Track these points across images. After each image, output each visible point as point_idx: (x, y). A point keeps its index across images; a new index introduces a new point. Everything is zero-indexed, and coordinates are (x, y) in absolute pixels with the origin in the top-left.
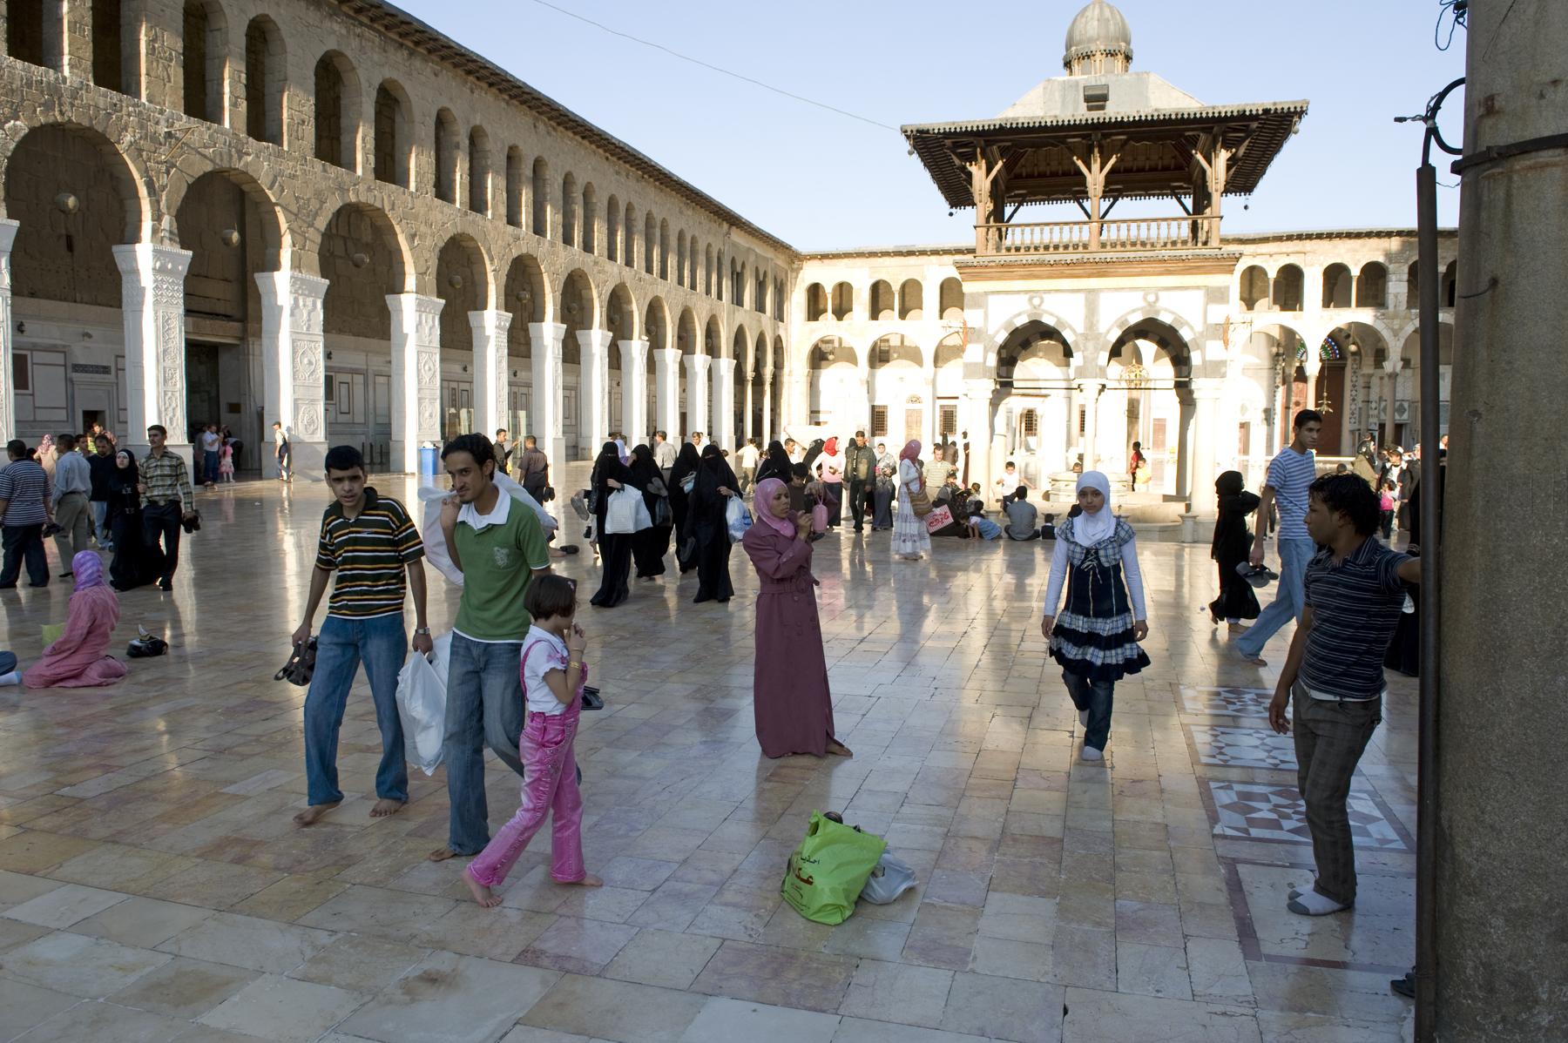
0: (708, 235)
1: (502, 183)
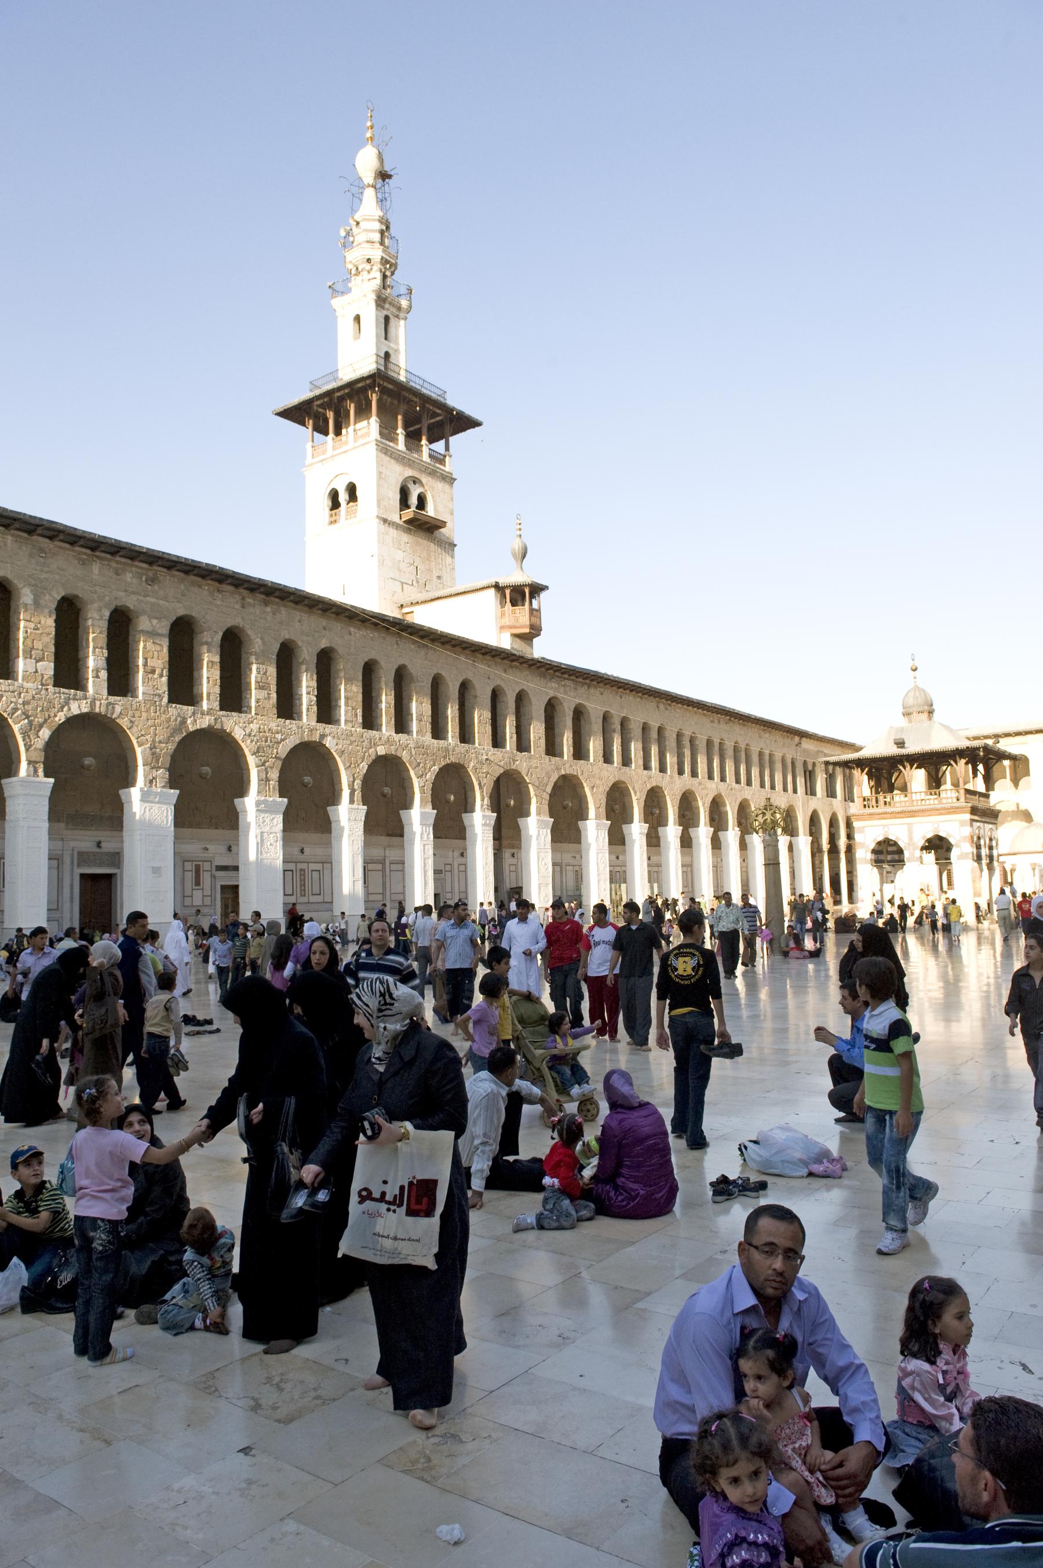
0: (781, 749)
1: (640, 746)
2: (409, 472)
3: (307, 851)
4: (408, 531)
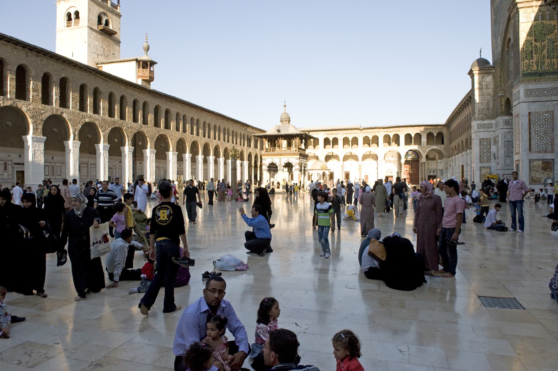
0: (240, 131)
1: (190, 126)
2: (102, 10)
3: (54, 158)
4: (101, 34)
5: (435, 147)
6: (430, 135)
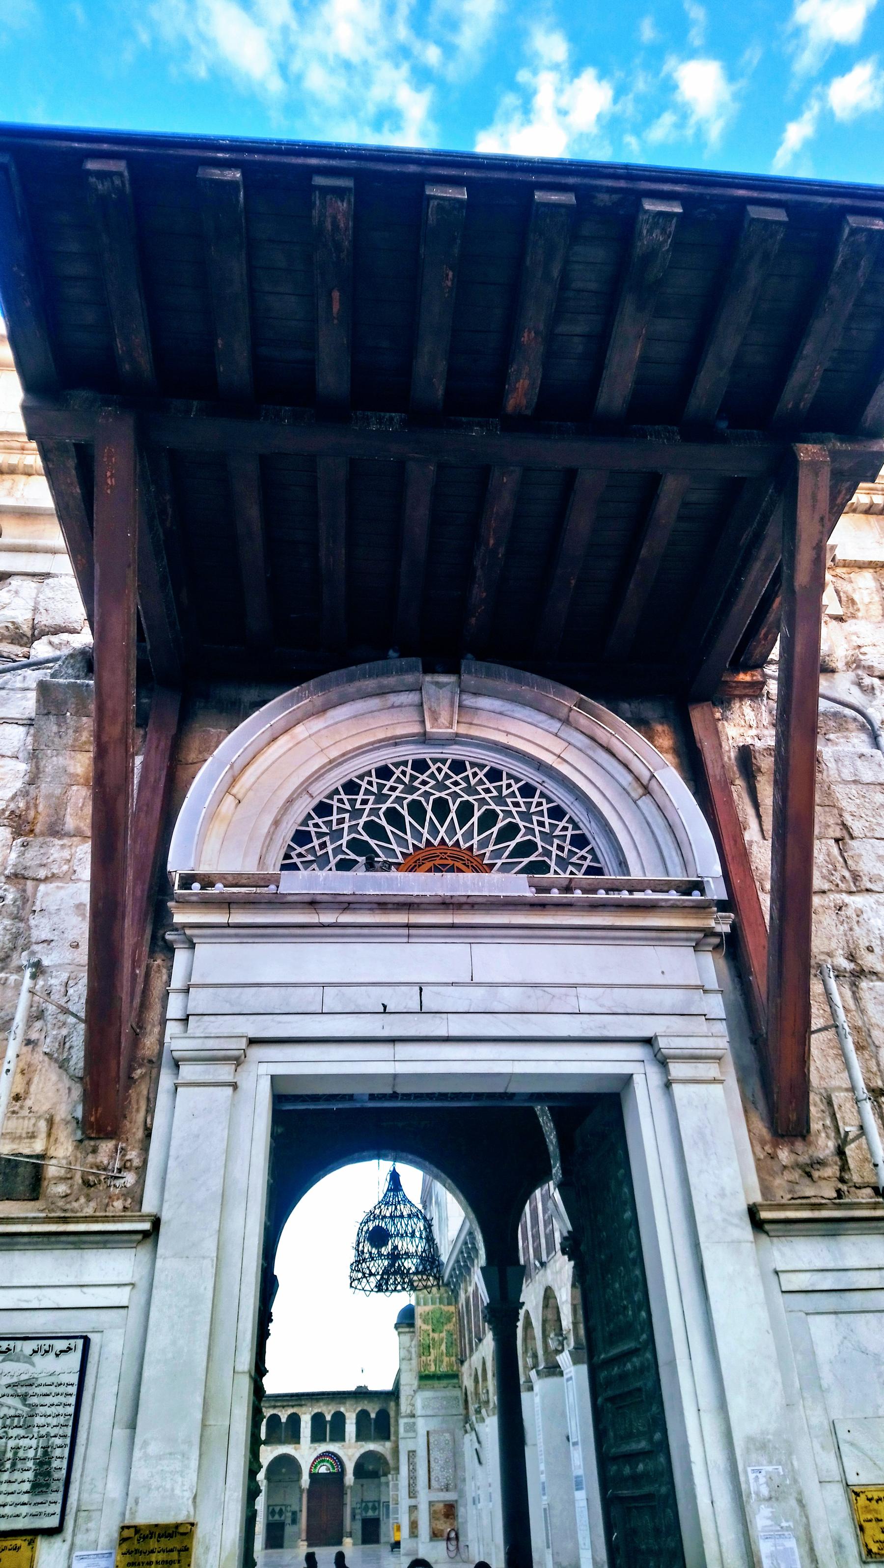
5: (371, 1446)
6: (362, 1416)
